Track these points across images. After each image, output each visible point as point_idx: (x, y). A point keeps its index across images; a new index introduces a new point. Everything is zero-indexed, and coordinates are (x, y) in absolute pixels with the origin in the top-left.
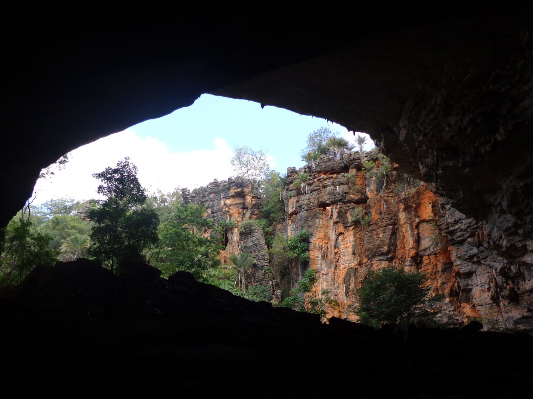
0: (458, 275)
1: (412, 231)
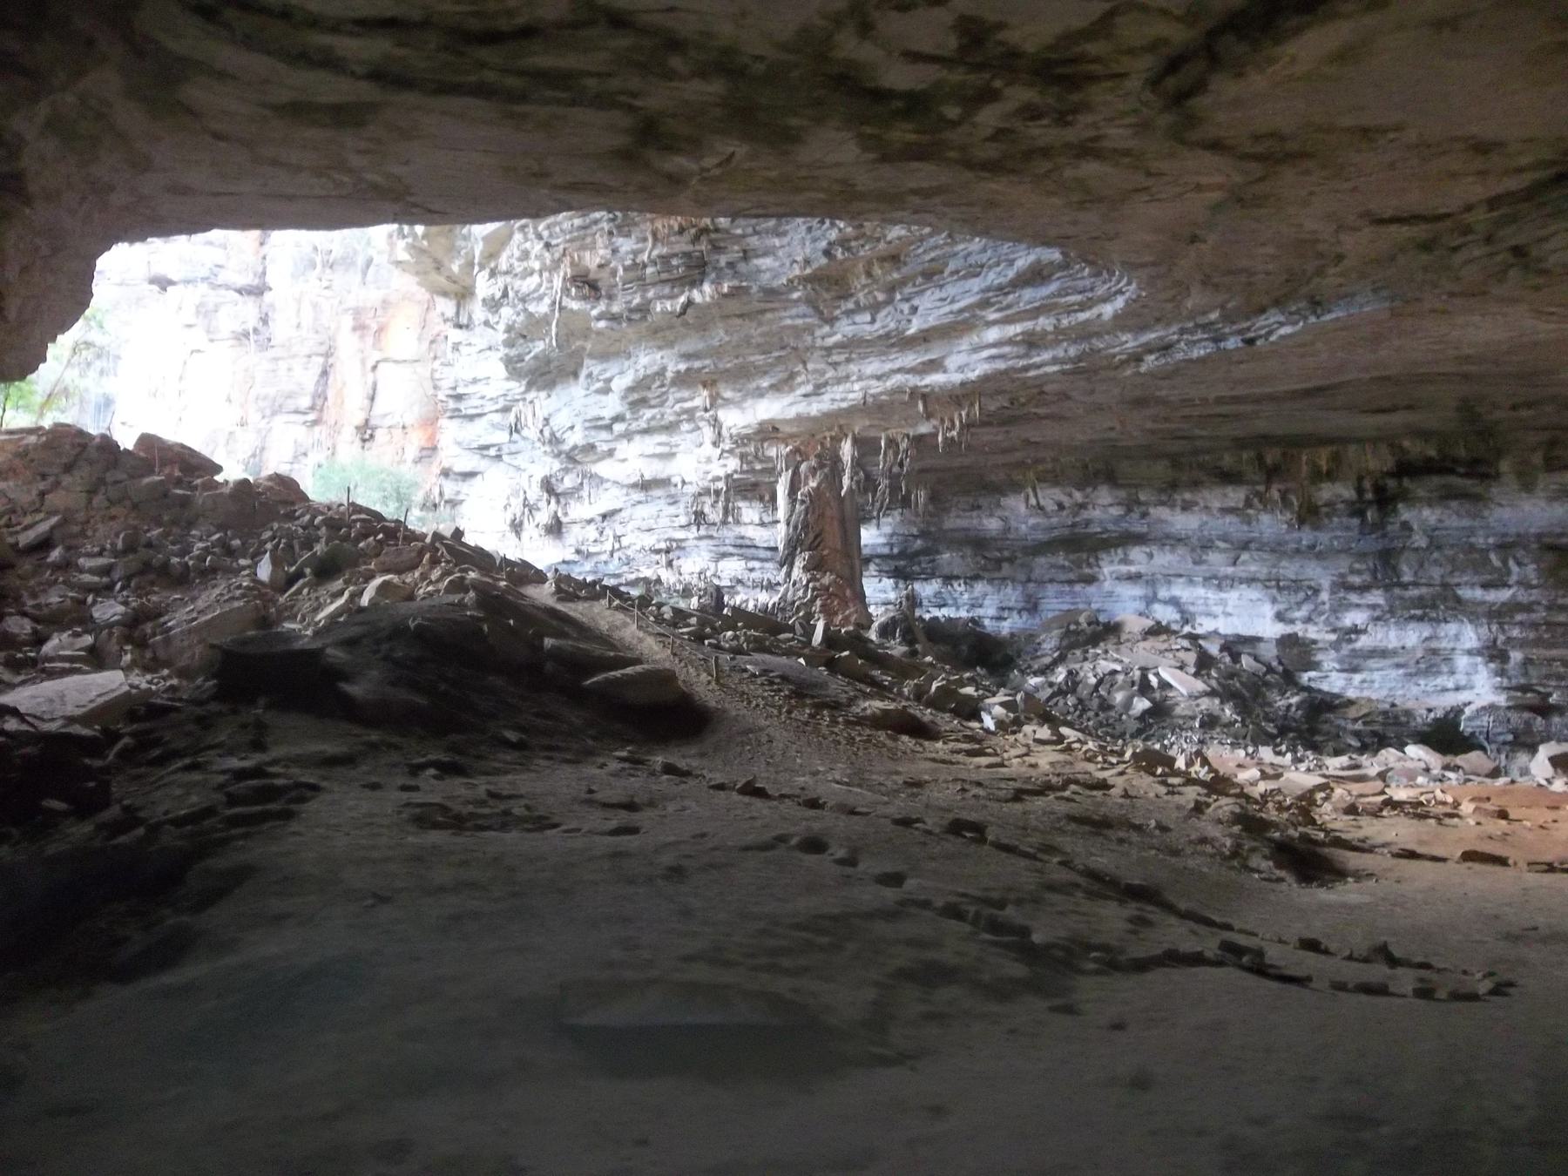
0: (446, 473)
1: (364, 375)
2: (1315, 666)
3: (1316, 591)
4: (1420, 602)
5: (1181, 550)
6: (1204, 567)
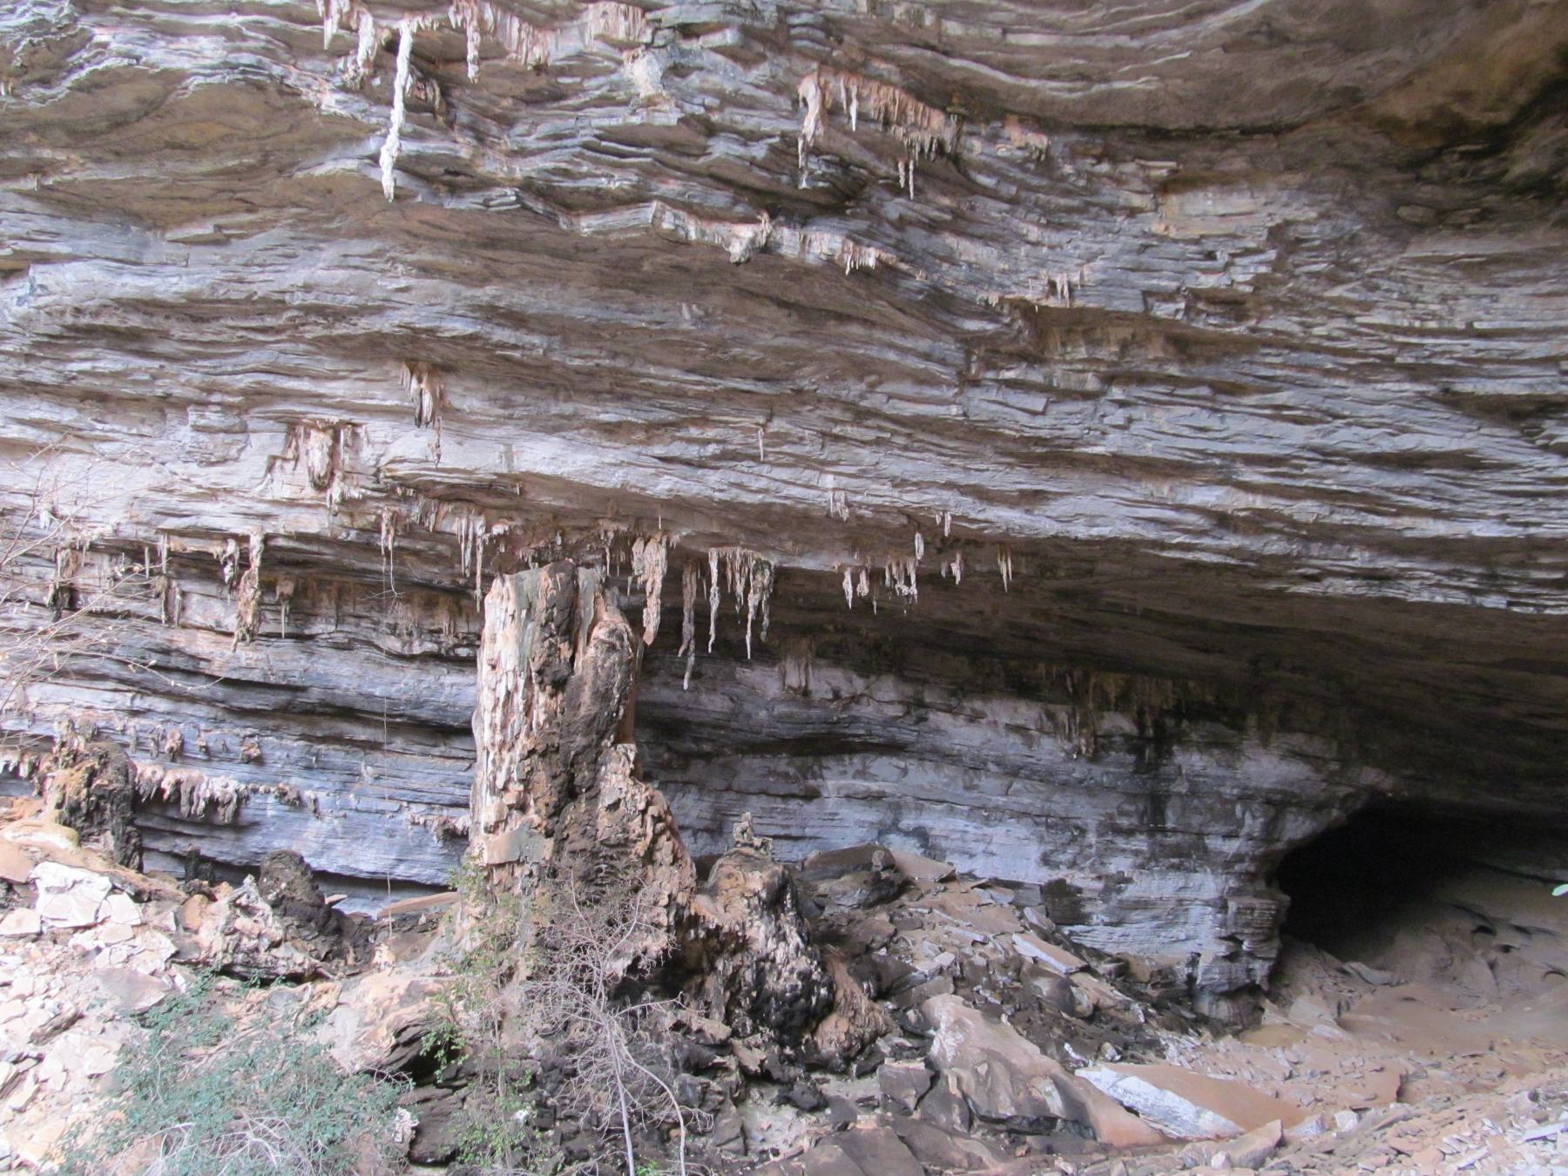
2: (1082, 919)
3: (1083, 832)
4: (1177, 851)
5: (949, 770)
6: (975, 794)
